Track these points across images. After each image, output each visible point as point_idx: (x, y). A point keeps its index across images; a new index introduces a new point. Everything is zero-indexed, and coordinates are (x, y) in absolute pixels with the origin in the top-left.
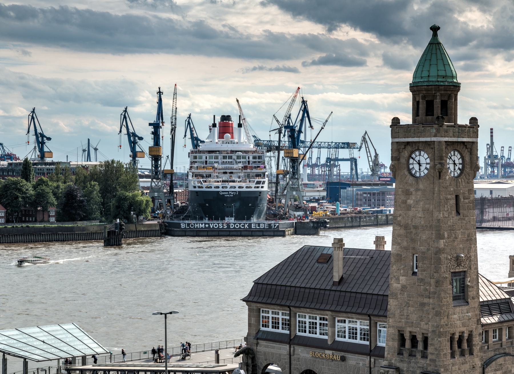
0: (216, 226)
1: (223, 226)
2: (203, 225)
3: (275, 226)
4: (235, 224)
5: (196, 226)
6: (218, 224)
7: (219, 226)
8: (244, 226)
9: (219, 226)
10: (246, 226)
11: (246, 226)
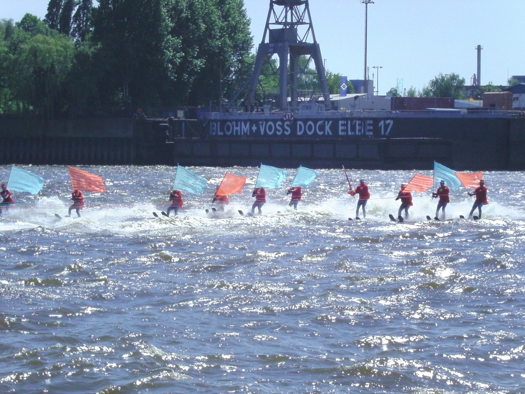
0: (270, 128)
1: (284, 130)
2: (248, 124)
3: (386, 126)
4: (305, 121)
5: (235, 128)
6: (275, 121)
7: (276, 130)
8: (322, 128)
9: (276, 130)
10: (327, 128)
11: (327, 128)
